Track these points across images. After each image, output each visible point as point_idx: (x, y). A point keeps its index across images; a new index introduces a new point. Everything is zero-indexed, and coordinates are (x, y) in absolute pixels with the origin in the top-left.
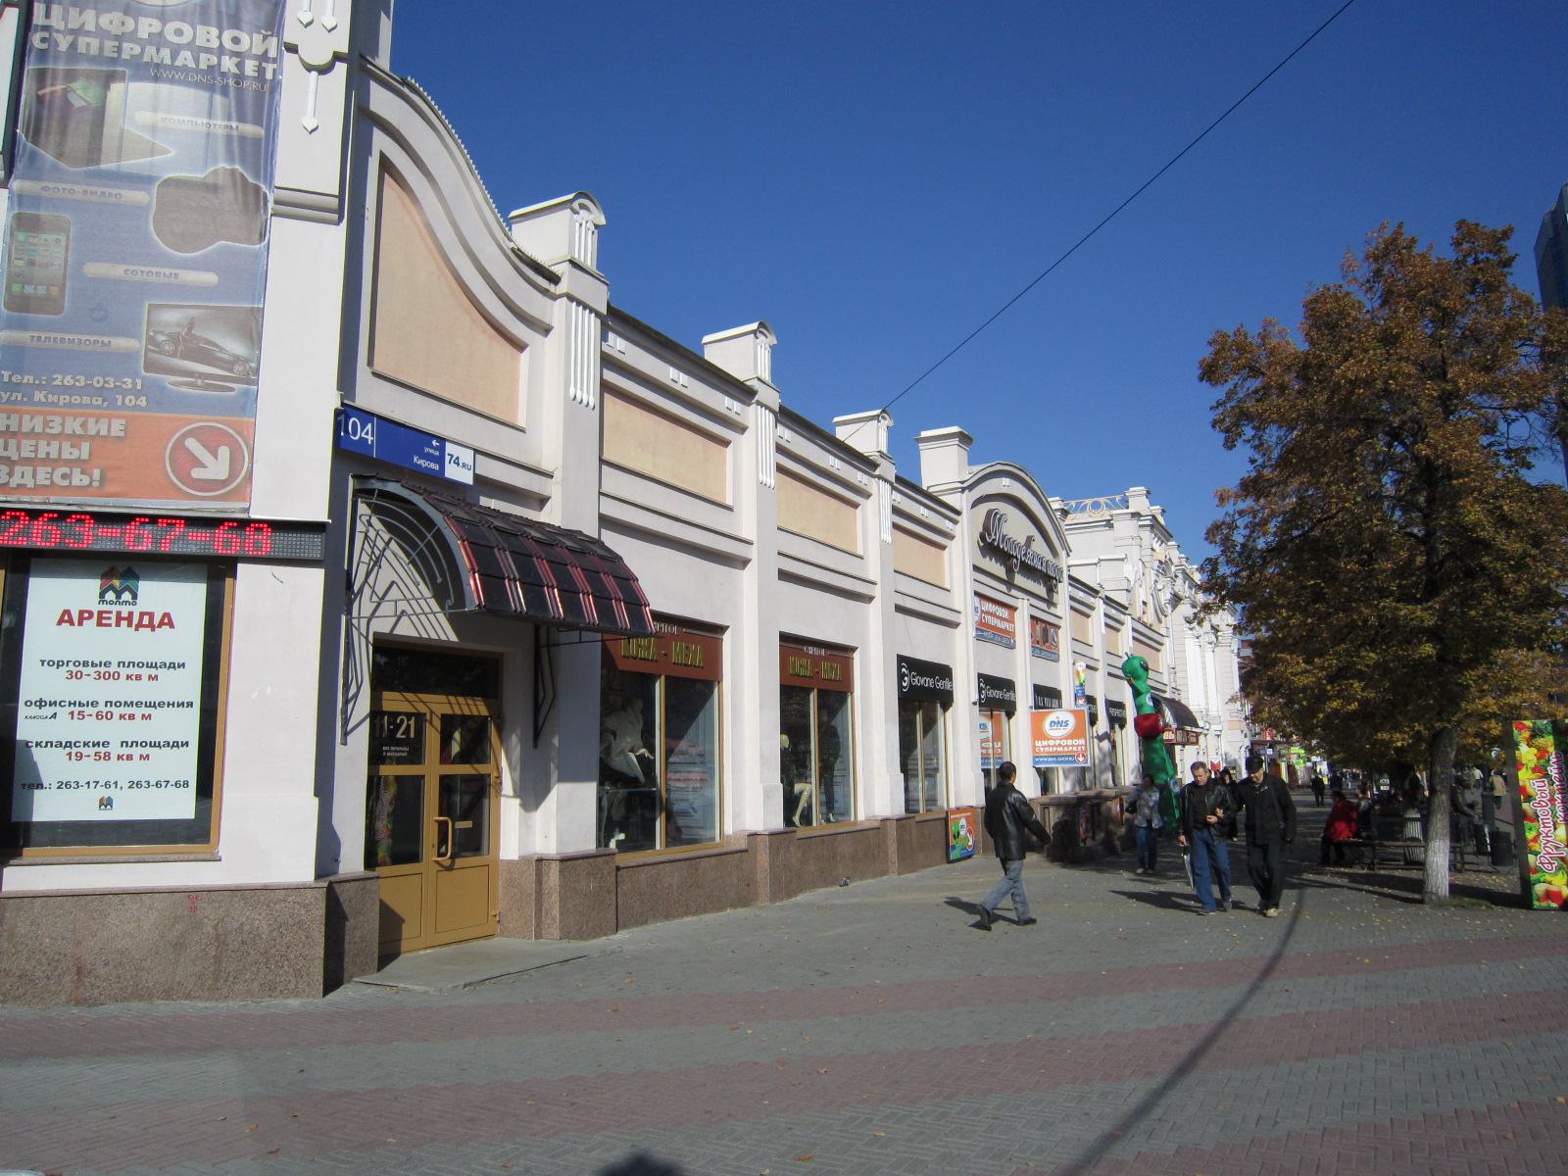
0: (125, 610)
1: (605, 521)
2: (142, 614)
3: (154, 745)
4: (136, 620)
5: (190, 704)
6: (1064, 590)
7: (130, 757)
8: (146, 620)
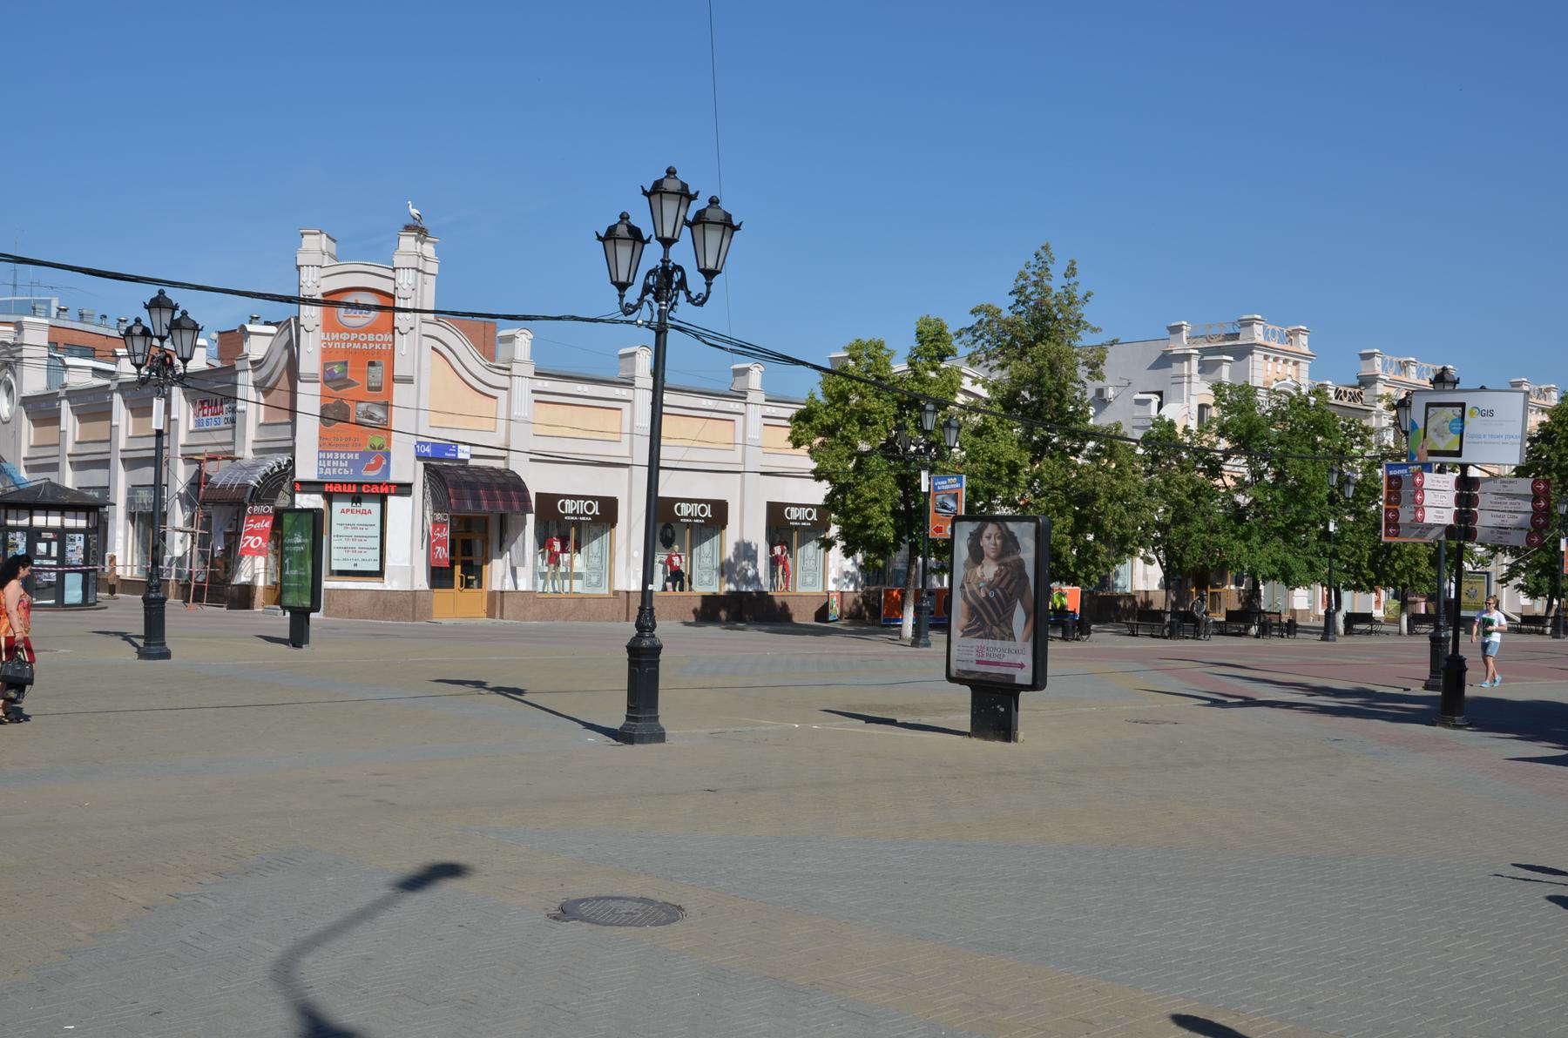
0: (358, 509)
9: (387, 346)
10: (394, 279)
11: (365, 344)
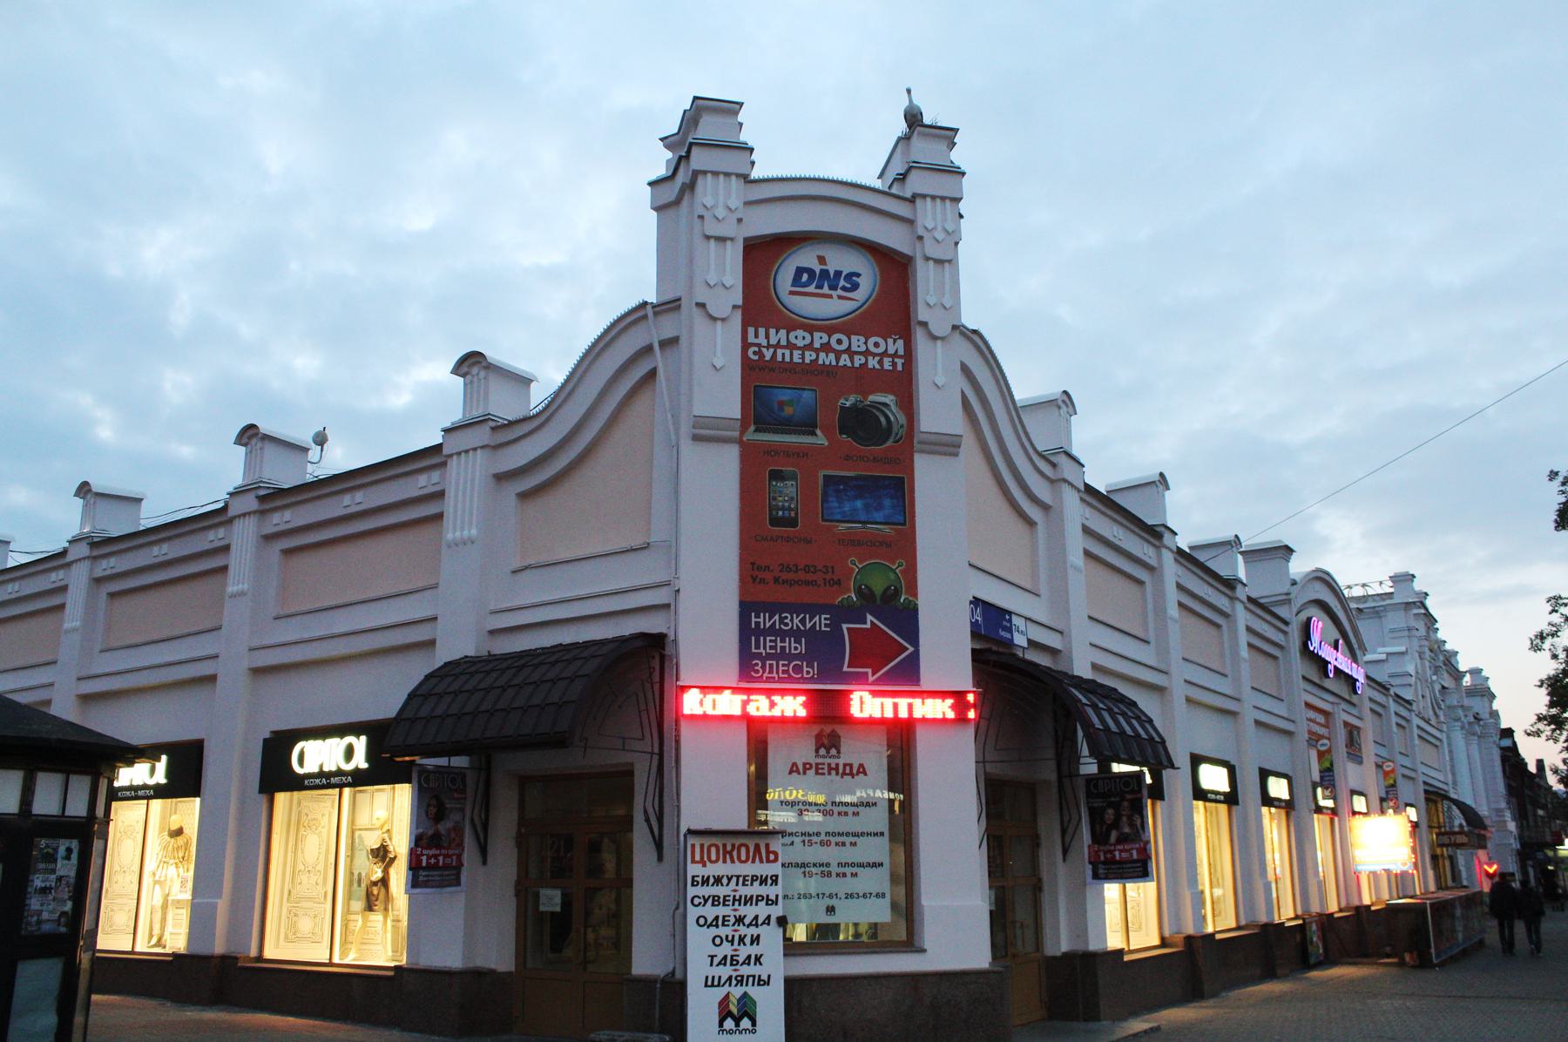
0: (833, 762)
1: (1095, 667)
2: (845, 765)
3: (861, 865)
4: (841, 771)
5: (882, 834)
7: (844, 875)
8: (848, 771)
9: (894, 364)
10: (910, 222)
11: (845, 356)
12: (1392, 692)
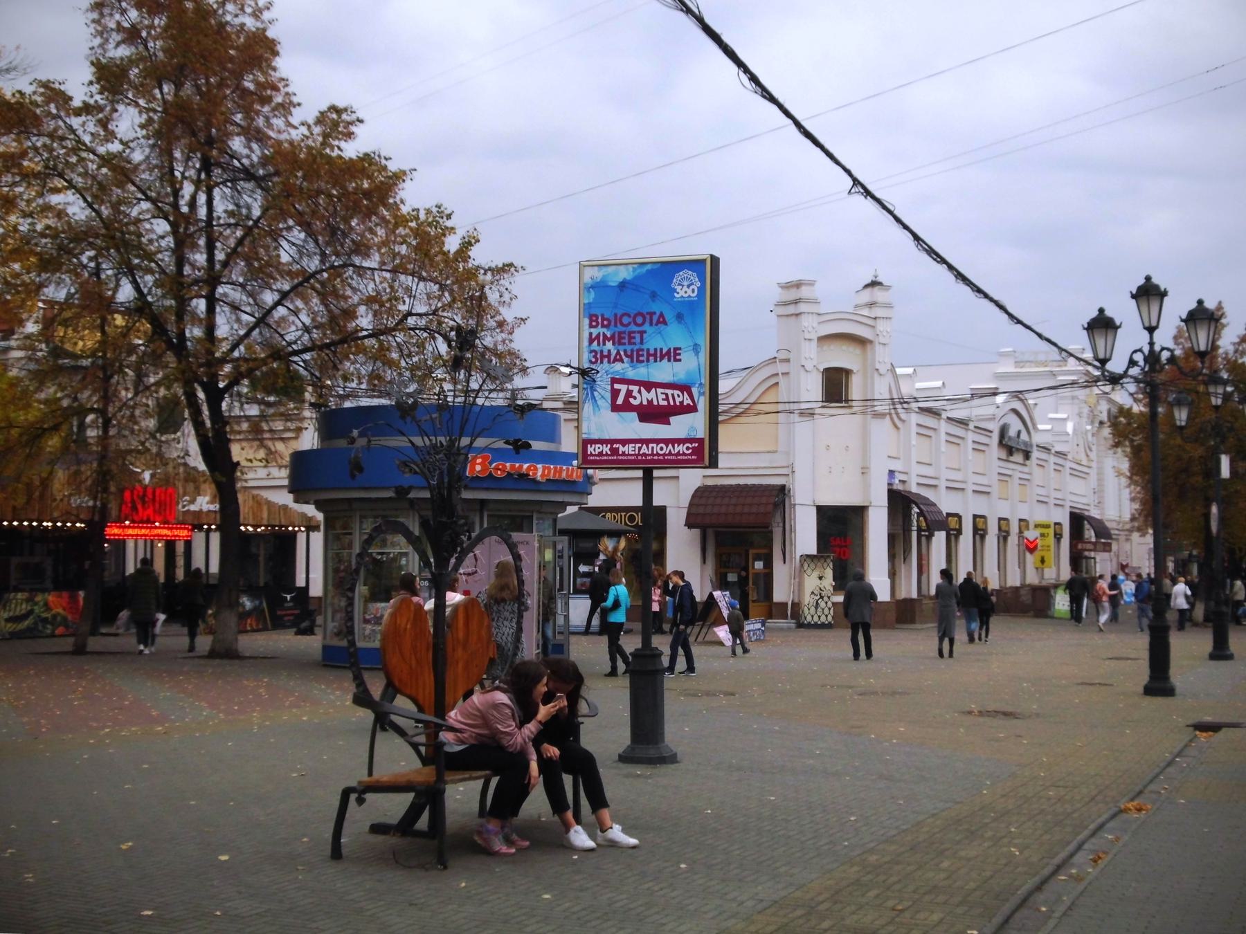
6: (1035, 454)
12: (1053, 451)
